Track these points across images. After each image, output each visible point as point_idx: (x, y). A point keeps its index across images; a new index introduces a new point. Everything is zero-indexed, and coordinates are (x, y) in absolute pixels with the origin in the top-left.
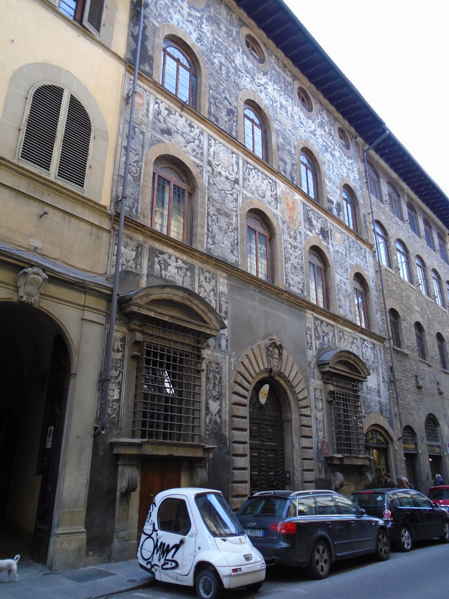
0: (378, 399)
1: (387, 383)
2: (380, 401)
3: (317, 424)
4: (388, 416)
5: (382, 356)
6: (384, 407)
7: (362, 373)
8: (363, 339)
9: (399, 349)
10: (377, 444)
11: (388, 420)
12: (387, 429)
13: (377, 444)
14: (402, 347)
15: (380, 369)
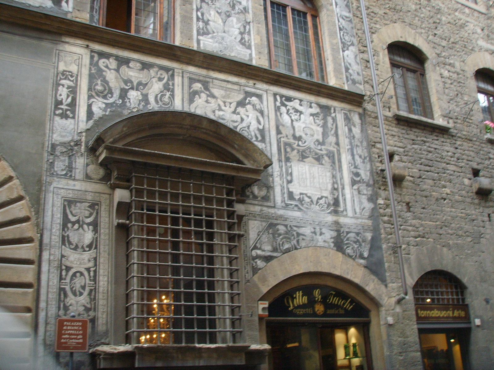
0: (330, 219)
1: (368, 185)
2: (337, 223)
3: (61, 279)
4: (366, 254)
5: (356, 131)
6: (352, 235)
7: (246, 162)
8: (282, 96)
9: (430, 121)
10: (325, 315)
11: (362, 261)
12: (357, 281)
13: (325, 315)
14: (436, 115)
15: (345, 158)
